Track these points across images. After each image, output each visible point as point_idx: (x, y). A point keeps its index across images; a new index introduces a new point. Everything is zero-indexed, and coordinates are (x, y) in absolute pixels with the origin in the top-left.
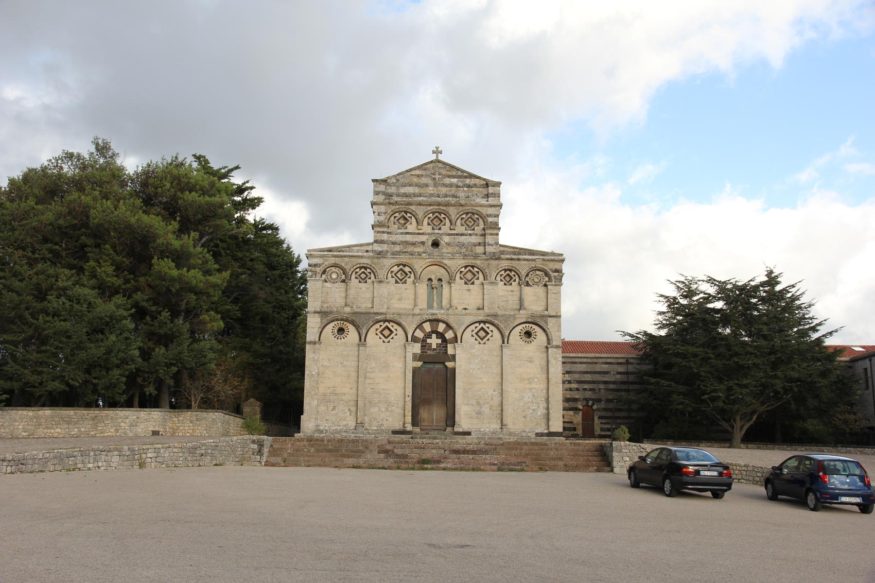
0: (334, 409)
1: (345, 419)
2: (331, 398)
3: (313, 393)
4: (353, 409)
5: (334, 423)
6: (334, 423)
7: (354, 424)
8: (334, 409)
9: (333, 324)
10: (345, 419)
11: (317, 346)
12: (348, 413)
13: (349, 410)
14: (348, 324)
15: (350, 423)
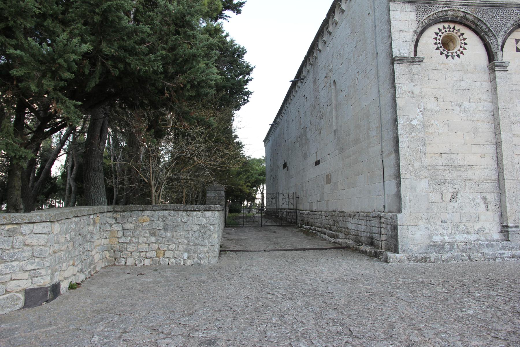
0: (454, 197)
1: (477, 219)
2: (447, 175)
3: (417, 165)
4: (492, 197)
5: (456, 226)
6: (456, 226)
7: (497, 228)
8: (454, 197)
9: (434, 29)
10: (477, 219)
11: (415, 68)
12: (482, 207)
13: (484, 198)
14: (463, 30)
15: (487, 225)
